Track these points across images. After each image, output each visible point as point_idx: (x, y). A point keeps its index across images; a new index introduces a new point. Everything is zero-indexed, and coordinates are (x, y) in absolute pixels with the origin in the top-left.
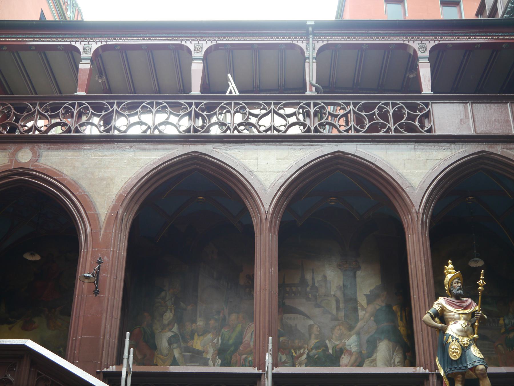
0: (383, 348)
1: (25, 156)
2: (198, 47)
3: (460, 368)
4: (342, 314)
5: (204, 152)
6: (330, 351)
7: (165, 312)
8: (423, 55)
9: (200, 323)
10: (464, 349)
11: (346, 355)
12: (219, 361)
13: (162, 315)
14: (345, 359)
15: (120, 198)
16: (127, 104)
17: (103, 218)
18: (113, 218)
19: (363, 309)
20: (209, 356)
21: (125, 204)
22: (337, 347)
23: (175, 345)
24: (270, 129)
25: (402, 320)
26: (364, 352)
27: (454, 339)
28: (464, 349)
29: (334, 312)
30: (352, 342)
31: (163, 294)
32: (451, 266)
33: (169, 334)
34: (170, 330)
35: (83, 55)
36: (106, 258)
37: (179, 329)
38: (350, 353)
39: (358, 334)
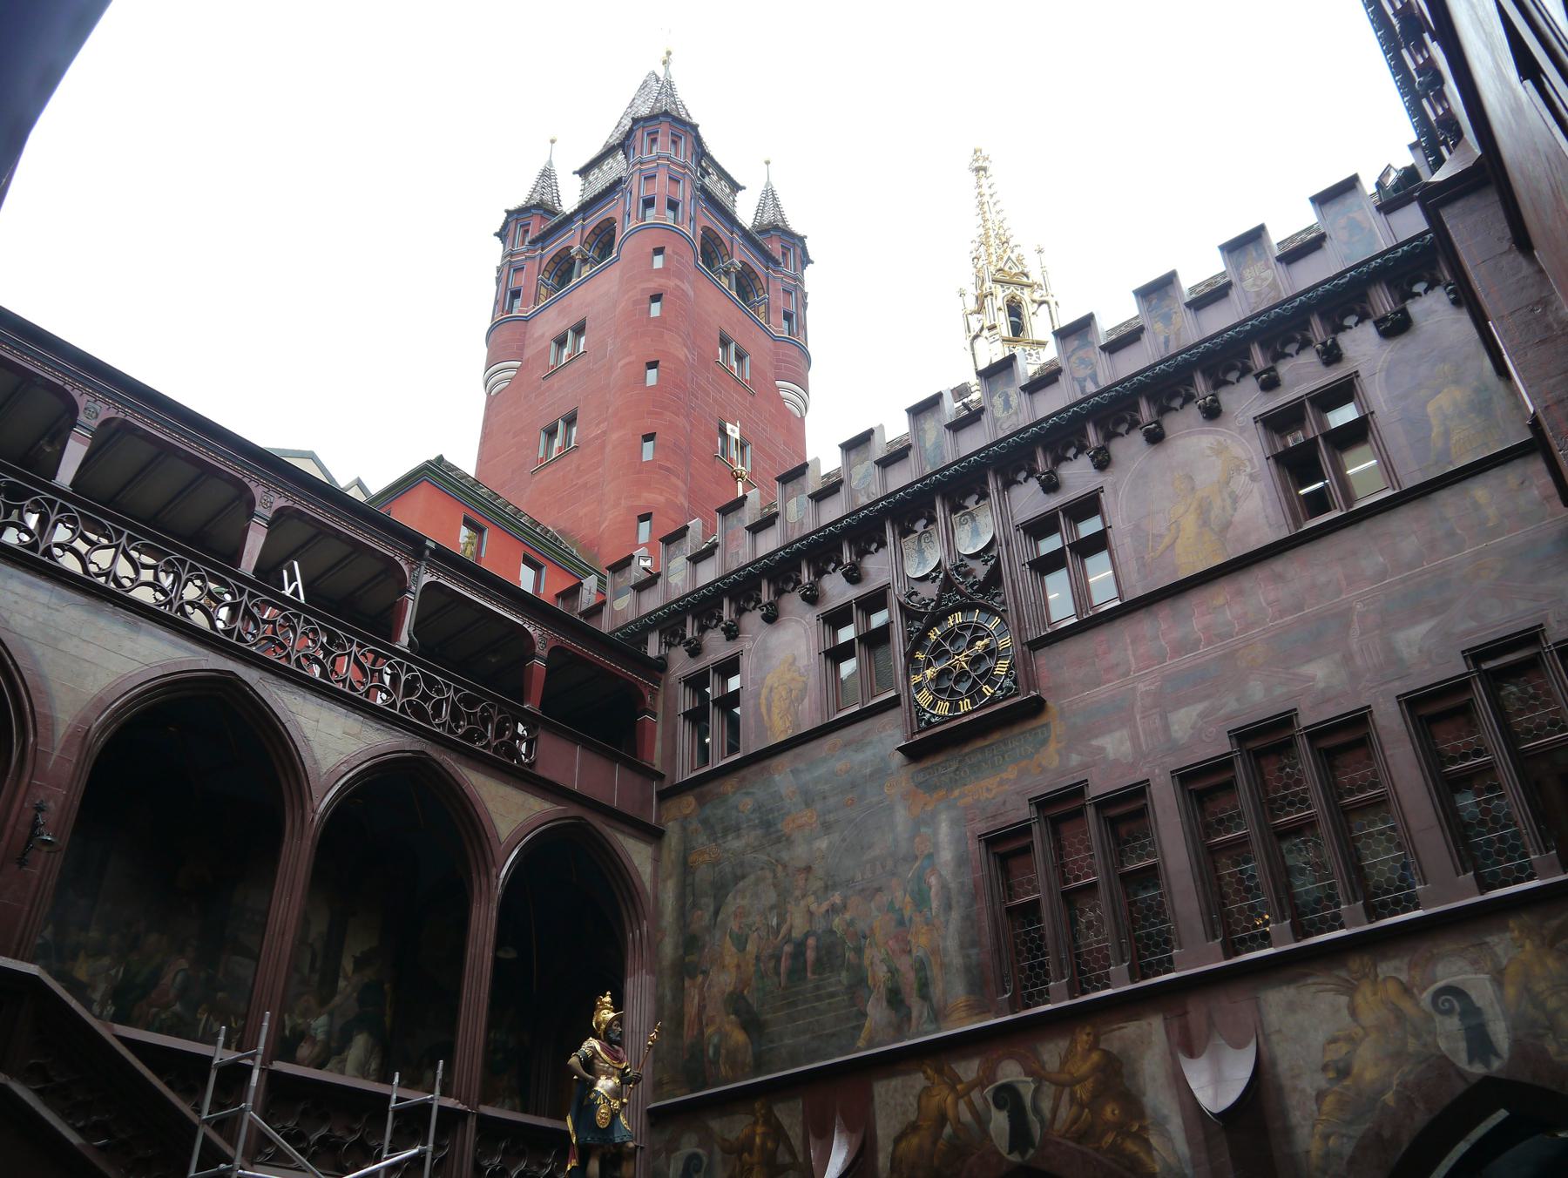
0: (359, 1045)
2: (269, 500)
4: (316, 977)
5: (246, 678)
8: (541, 650)
9: (94, 934)
12: (111, 1009)
14: (304, 1051)
15: (99, 704)
16: (144, 545)
17: (61, 731)
18: (80, 736)
19: (346, 978)
20: (97, 996)
24: (344, 681)
26: (333, 1045)
28: (614, 1116)
29: (306, 971)
30: (319, 1025)
32: (608, 999)
36: (51, 804)
38: (314, 1041)
39: (331, 1015)
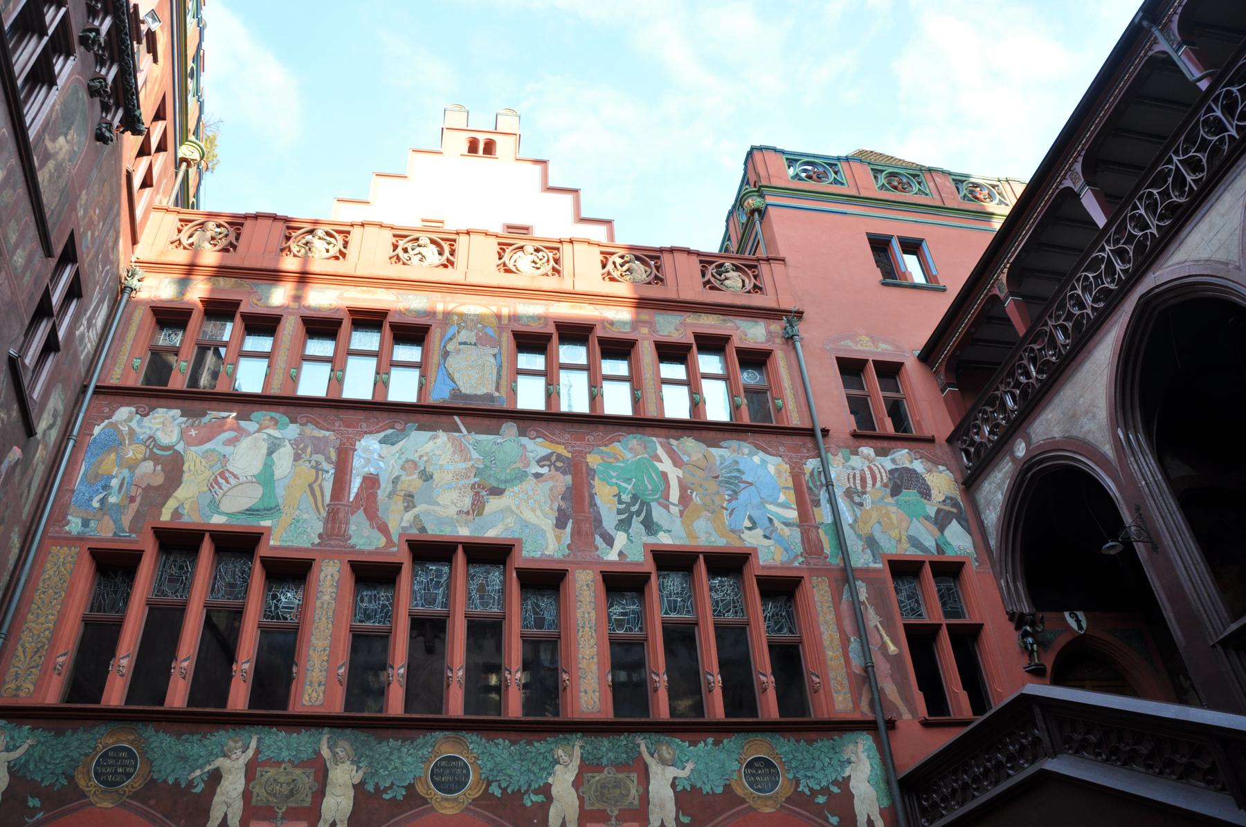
1: (1021, 450)
21: (1121, 422)
35: (1002, 296)
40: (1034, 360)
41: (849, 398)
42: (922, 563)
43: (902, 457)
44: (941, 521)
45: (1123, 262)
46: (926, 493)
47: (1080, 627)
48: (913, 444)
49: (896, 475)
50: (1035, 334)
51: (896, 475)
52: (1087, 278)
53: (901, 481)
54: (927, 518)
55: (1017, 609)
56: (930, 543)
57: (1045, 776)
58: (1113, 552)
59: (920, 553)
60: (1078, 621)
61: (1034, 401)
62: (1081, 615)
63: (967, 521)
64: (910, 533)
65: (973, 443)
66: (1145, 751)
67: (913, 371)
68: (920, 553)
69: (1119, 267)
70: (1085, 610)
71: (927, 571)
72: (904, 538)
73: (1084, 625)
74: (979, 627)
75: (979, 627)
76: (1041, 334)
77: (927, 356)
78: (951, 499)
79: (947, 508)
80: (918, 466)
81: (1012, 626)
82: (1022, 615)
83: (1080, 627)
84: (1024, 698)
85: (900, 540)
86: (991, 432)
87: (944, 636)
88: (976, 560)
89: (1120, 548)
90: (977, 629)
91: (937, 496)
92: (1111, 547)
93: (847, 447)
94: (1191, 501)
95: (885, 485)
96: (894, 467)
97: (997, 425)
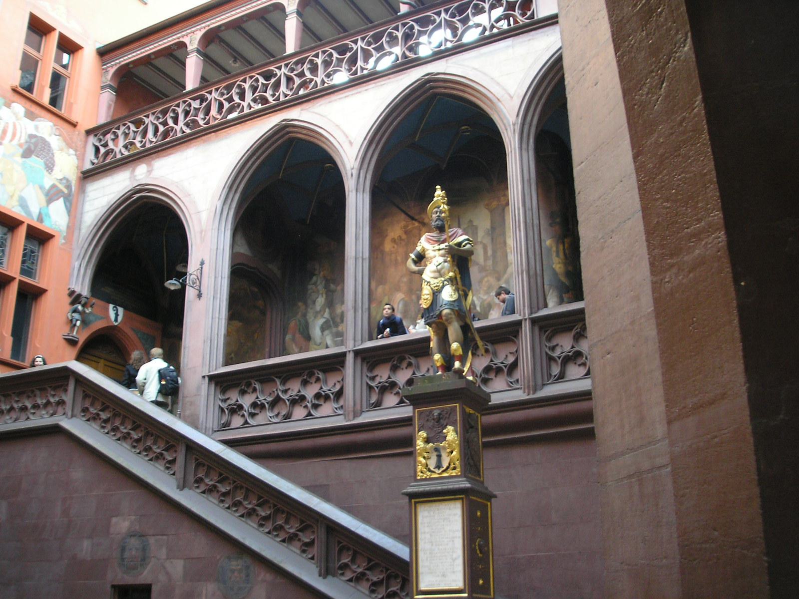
3: (432, 316)
6: (478, 309)
7: (317, 298)
10: (436, 293)
11: (495, 309)
13: (314, 302)
22: (486, 303)
23: (326, 332)
25: (558, 255)
27: (426, 283)
28: (436, 293)
31: (314, 278)
33: (321, 321)
34: (322, 316)
35: (190, 48)
37: (331, 314)
40: (187, 113)
41: (26, 56)
42: (22, 222)
43: (45, 127)
44: (51, 195)
45: (287, 88)
46: (50, 167)
47: (116, 320)
48: (60, 122)
49: (33, 140)
50: (198, 95)
51: (33, 140)
52: (257, 80)
53: (34, 148)
54: (41, 188)
55: (78, 290)
56: (35, 210)
57: (56, 430)
58: (172, 288)
59: (23, 213)
60: (117, 315)
61: (168, 144)
62: (121, 311)
63: (71, 204)
64: (23, 194)
65: (105, 145)
66: (136, 437)
67: (88, 57)
68: (23, 213)
69: (283, 88)
70: (125, 308)
71: (22, 232)
72: (16, 198)
73: (120, 319)
74: (44, 291)
75: (44, 291)
76: (202, 99)
77: (105, 53)
78: (68, 180)
79: (61, 187)
80: (55, 142)
81: (69, 300)
82: (79, 296)
83: (116, 320)
84: (66, 369)
85: (12, 197)
86: (126, 147)
87: (14, 289)
88: (65, 238)
89: (179, 287)
90: (39, 292)
91: (58, 173)
92: (172, 284)
93: (4, 97)
94: (238, 272)
95: (21, 145)
96: (34, 133)
97: (132, 144)
